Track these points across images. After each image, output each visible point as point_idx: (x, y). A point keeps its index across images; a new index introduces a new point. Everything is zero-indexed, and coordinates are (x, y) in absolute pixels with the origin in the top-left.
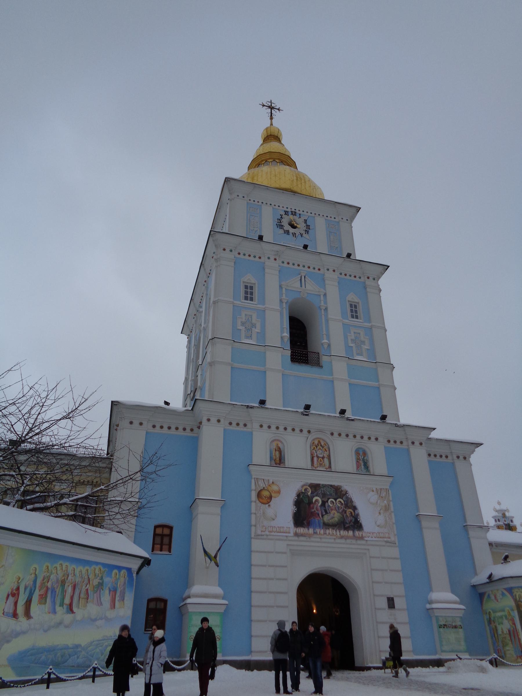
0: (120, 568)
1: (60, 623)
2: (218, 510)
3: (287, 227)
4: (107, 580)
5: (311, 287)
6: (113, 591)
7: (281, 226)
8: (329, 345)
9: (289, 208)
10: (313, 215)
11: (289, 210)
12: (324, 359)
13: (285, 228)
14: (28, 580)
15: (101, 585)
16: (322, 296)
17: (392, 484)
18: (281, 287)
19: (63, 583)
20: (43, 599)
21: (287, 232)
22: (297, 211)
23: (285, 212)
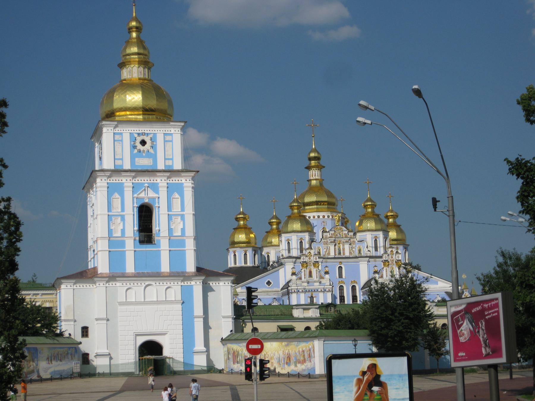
0: (72, 348)
1: (59, 365)
2: (105, 322)
3: (139, 146)
4: (69, 352)
5: (151, 194)
6: (71, 354)
7: (135, 147)
8: (159, 230)
9: (141, 130)
10: (156, 132)
11: (141, 132)
12: (156, 238)
13: (138, 148)
14: (50, 355)
15: (68, 354)
16: (157, 199)
17: (183, 303)
18: (133, 198)
19: (58, 354)
20: (54, 359)
21: (139, 151)
22: (146, 132)
23: (139, 134)
